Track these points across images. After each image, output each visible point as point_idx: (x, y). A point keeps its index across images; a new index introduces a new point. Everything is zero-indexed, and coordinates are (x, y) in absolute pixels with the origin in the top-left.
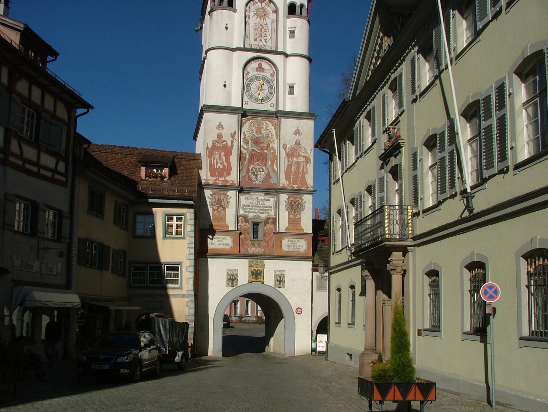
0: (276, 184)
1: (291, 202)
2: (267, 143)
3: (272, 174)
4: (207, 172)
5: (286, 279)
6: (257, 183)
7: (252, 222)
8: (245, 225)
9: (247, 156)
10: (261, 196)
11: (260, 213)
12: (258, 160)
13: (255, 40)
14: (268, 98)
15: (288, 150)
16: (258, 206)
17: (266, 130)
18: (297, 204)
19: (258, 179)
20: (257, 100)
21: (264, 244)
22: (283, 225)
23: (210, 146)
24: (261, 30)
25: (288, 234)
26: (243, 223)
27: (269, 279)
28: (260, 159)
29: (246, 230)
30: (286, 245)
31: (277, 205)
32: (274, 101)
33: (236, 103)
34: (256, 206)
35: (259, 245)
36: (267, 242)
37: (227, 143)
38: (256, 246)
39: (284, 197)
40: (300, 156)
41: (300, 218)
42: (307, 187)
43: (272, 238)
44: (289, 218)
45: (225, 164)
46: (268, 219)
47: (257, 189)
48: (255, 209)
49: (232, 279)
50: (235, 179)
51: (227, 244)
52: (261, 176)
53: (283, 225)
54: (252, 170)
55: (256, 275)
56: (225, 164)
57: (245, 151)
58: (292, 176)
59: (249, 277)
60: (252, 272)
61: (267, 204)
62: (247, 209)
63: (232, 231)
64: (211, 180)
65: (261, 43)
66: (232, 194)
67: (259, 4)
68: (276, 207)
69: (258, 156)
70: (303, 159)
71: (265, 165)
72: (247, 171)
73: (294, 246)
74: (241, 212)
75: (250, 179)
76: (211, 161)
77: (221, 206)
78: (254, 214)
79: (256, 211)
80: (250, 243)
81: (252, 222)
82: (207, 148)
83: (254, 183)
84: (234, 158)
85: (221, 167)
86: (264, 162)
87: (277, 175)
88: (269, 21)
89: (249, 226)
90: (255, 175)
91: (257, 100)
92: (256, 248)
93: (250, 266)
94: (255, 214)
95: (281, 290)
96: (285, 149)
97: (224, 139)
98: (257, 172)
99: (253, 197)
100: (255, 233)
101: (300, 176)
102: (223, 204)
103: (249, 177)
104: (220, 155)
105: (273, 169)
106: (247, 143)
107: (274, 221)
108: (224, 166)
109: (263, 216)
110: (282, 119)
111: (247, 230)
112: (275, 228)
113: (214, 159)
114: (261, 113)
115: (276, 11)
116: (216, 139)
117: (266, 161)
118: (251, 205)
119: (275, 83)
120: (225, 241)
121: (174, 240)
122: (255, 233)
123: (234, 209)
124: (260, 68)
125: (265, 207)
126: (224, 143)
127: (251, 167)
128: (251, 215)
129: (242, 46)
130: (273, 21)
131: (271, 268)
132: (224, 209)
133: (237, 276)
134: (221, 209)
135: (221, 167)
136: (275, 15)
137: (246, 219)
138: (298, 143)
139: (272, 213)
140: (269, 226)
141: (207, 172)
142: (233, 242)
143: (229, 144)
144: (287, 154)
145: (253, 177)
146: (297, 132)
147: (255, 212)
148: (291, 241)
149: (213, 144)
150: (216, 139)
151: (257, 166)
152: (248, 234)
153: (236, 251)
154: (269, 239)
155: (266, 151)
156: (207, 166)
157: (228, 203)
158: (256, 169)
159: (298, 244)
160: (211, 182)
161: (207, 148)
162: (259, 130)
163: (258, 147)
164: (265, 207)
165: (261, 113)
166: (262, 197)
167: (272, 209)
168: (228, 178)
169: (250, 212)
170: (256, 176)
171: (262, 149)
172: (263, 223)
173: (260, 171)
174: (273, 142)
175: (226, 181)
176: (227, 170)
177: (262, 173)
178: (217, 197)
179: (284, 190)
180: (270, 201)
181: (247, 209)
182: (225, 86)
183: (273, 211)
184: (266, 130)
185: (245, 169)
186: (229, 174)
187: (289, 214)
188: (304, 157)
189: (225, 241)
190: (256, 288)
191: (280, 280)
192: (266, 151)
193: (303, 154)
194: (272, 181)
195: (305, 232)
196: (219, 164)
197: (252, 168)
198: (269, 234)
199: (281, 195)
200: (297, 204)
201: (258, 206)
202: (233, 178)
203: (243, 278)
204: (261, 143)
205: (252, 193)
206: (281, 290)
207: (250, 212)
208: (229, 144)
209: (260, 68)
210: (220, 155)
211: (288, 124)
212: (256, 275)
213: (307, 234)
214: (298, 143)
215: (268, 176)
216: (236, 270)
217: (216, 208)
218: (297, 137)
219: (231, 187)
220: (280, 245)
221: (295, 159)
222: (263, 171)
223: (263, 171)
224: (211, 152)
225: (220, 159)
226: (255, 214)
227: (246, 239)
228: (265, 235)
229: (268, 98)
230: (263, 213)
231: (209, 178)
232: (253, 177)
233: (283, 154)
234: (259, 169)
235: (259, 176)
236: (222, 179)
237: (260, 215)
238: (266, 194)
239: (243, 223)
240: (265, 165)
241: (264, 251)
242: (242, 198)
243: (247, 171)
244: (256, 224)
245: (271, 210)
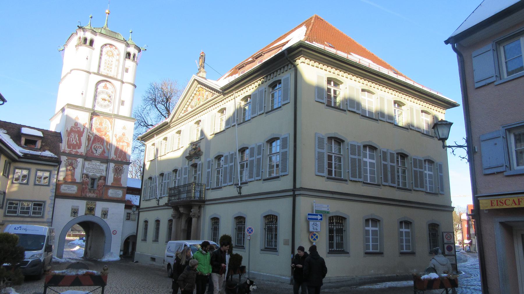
0: (108, 157)
3: (106, 151)
5: (109, 214)
10: (98, 163)
12: (99, 142)
13: (105, 69)
14: (108, 105)
20: (101, 106)
21: (97, 192)
22: (110, 181)
23: (69, 130)
24: (109, 64)
25: (112, 187)
27: (98, 213)
29: (87, 183)
30: (111, 193)
31: (107, 169)
32: (111, 108)
33: (89, 105)
35: (94, 192)
36: (99, 191)
38: (92, 192)
39: (112, 165)
40: (124, 142)
41: (120, 178)
42: (127, 160)
45: (78, 142)
46: (101, 177)
47: (96, 159)
49: (75, 212)
50: (83, 151)
52: (100, 151)
53: (110, 181)
55: (91, 210)
56: (78, 142)
57: (91, 135)
59: (86, 211)
60: (88, 208)
61: (102, 168)
63: (77, 183)
64: (67, 150)
65: (108, 72)
66: (80, 160)
67: (109, 48)
70: (125, 144)
71: (103, 145)
72: (91, 147)
74: (85, 172)
75: (92, 152)
76: (68, 139)
80: (88, 190)
82: (67, 131)
84: (84, 139)
85: (75, 143)
87: (109, 152)
88: (114, 60)
89: (89, 180)
91: (101, 106)
93: (87, 204)
95: (105, 220)
96: (116, 137)
97: (79, 126)
99: (93, 163)
100: (93, 184)
104: (75, 136)
105: (107, 148)
107: (105, 178)
108: (77, 143)
109: (98, 175)
112: (105, 183)
114: (103, 114)
115: (118, 55)
116: (73, 125)
119: (113, 97)
120: (72, 189)
121: (42, 187)
122: (93, 184)
123: (80, 170)
124: (105, 87)
127: (94, 145)
128: (91, 174)
129: (96, 71)
130: (117, 60)
131: (100, 207)
133: (78, 210)
135: (75, 143)
136: (118, 57)
137: (87, 176)
138: (124, 135)
139: (104, 174)
140: (101, 181)
143: (82, 130)
144: (117, 140)
145: (95, 152)
146: (124, 128)
149: (71, 129)
150: (73, 125)
151: (97, 145)
153: (79, 195)
157: (77, 165)
159: (118, 193)
160: (67, 152)
161: (67, 131)
162: (101, 124)
165: (103, 114)
166: (99, 164)
168: (78, 150)
170: (97, 151)
175: (77, 152)
176: (79, 146)
178: (70, 161)
179: (113, 161)
180: (104, 166)
182: (82, 94)
185: (90, 146)
186: (79, 148)
187: (114, 175)
189: (72, 189)
190: (89, 218)
191: (105, 214)
194: (106, 155)
196: (74, 141)
199: (111, 164)
202: (82, 150)
203: (82, 212)
206: (105, 220)
208: (82, 130)
209: (105, 87)
210: (75, 136)
211: (119, 123)
212: (91, 210)
213: (124, 188)
214: (124, 135)
215: (104, 151)
219: (81, 156)
220: (107, 192)
224: (69, 133)
227: (86, 188)
228: (98, 186)
229: (108, 105)
231: (67, 149)
232: (95, 152)
236: (75, 150)
238: (101, 162)
241: (96, 196)
242: (87, 163)
243: (91, 147)
244: (93, 180)
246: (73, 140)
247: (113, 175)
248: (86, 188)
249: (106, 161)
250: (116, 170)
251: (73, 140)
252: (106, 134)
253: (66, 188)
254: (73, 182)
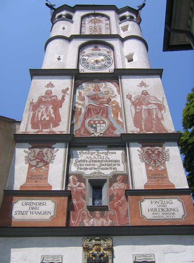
1: (147, 152)
2: (108, 98)
4: (27, 125)
6: (97, 135)
7: (90, 181)
8: (79, 186)
9: (83, 111)
11: (103, 169)
12: (98, 113)
15: (133, 99)
16: (99, 161)
17: (104, 88)
18: (156, 152)
19: (98, 131)
26: (75, 184)
28: (99, 113)
30: (150, 210)
31: (127, 158)
34: (95, 161)
36: (117, 209)
37: (57, 98)
39: (135, 151)
41: (165, 170)
43: (123, 202)
44: (148, 171)
48: (94, 165)
51: (45, 213)
54: (89, 122)
56: (53, 116)
58: (144, 123)
62: (81, 165)
66: (60, 152)
68: (126, 161)
69: (96, 110)
71: (107, 117)
73: (163, 210)
76: (34, 115)
77: (43, 161)
78: (93, 171)
79: (96, 167)
80: (85, 211)
81: (90, 181)
83: (93, 135)
86: (105, 115)
87: (122, 127)
90: (92, 127)
92: (98, 219)
94: (95, 171)
98: (96, 124)
101: (154, 122)
102: (45, 159)
103: (86, 129)
104: (47, 109)
105: (118, 121)
106: (83, 99)
107: (125, 178)
108: (51, 118)
109: (108, 172)
110: (123, 76)
111: (81, 193)
112: (128, 187)
113: (39, 111)
116: (44, 94)
117: (107, 114)
118: (87, 159)
119: (112, 57)
125: (110, 161)
126: (53, 98)
129: (78, 33)
132: (46, 164)
134: (41, 164)
135: (47, 119)
137: (80, 177)
139: (121, 168)
141: (27, 125)
142: (57, 208)
144: (133, 103)
147: (95, 169)
148: (156, 202)
151: (96, 118)
152: (84, 197)
154: (120, 205)
155: (106, 105)
156: (28, 118)
157: (53, 157)
158: (94, 121)
163: (96, 102)
164: (110, 161)
167: (121, 163)
169: (87, 169)
170: (95, 128)
171: (101, 104)
172: (108, 182)
173: (99, 123)
174: (114, 97)
176: (57, 121)
177: (102, 125)
181: (81, 165)
183: (122, 165)
184: (104, 88)
187: (147, 165)
188: (155, 104)
192: (106, 105)
193: (153, 102)
195: (176, 188)
196: (45, 116)
197: (90, 121)
198: (119, 197)
200: (156, 152)
201: (99, 161)
204: (100, 98)
205: (89, 147)
207: (87, 169)
211: (131, 85)
214: (145, 93)
216: (58, 256)
217: (34, 163)
218: (143, 88)
221: (144, 107)
222: (104, 123)
223: (104, 123)
225: (46, 111)
226: (95, 171)
227: (81, 206)
228: (111, 197)
230: (107, 169)
233: (128, 103)
234: (99, 121)
235: (98, 129)
237: (102, 171)
239: (75, 184)
240: (107, 117)
245: (119, 165)
246: (42, 115)
247: (143, 165)
248: (81, 206)
249: (121, 142)
250: (150, 155)
251: (42, 115)
252: (109, 101)
253: (26, 208)
254: (48, 194)
